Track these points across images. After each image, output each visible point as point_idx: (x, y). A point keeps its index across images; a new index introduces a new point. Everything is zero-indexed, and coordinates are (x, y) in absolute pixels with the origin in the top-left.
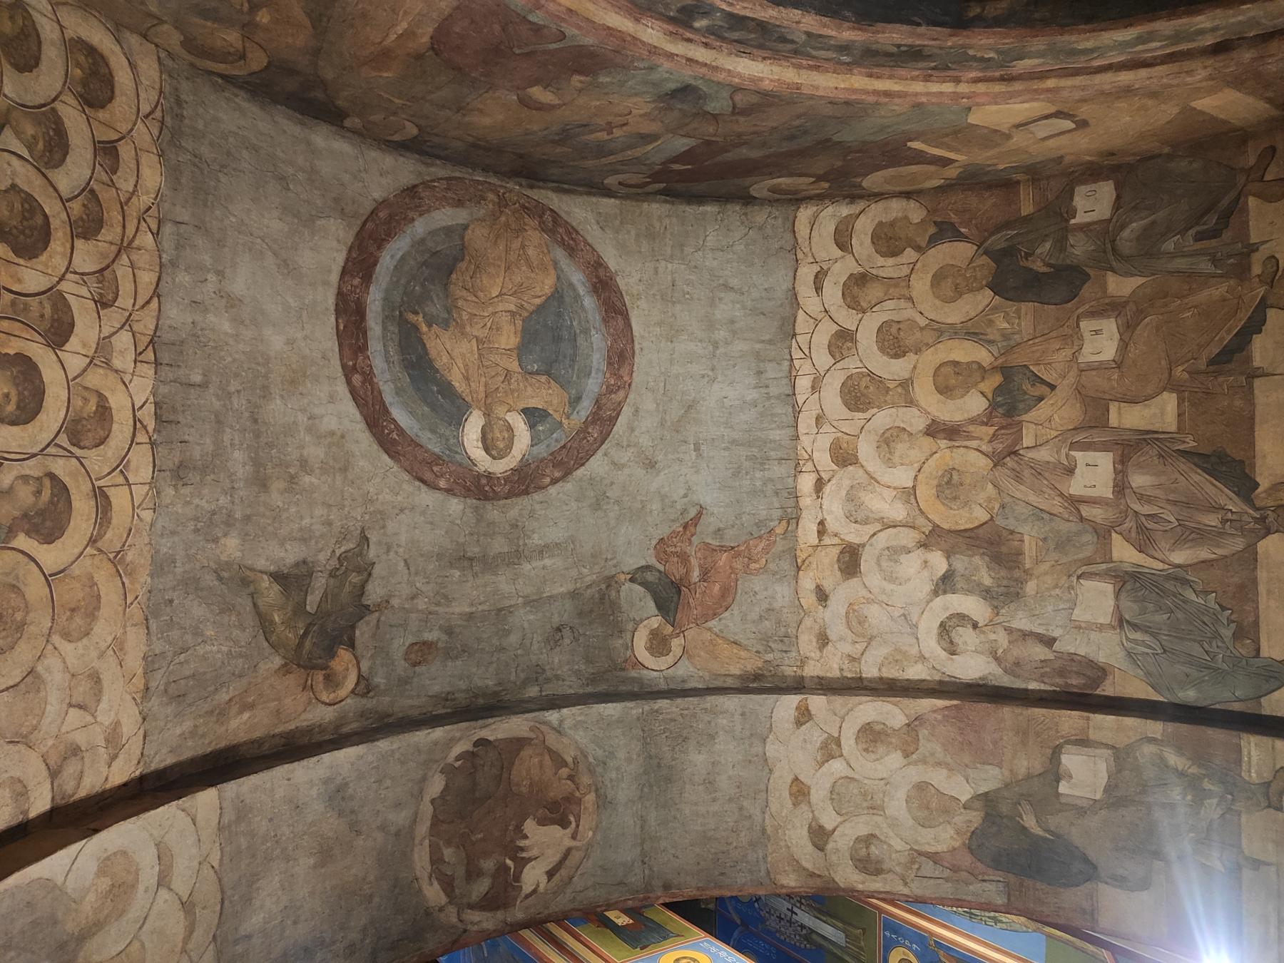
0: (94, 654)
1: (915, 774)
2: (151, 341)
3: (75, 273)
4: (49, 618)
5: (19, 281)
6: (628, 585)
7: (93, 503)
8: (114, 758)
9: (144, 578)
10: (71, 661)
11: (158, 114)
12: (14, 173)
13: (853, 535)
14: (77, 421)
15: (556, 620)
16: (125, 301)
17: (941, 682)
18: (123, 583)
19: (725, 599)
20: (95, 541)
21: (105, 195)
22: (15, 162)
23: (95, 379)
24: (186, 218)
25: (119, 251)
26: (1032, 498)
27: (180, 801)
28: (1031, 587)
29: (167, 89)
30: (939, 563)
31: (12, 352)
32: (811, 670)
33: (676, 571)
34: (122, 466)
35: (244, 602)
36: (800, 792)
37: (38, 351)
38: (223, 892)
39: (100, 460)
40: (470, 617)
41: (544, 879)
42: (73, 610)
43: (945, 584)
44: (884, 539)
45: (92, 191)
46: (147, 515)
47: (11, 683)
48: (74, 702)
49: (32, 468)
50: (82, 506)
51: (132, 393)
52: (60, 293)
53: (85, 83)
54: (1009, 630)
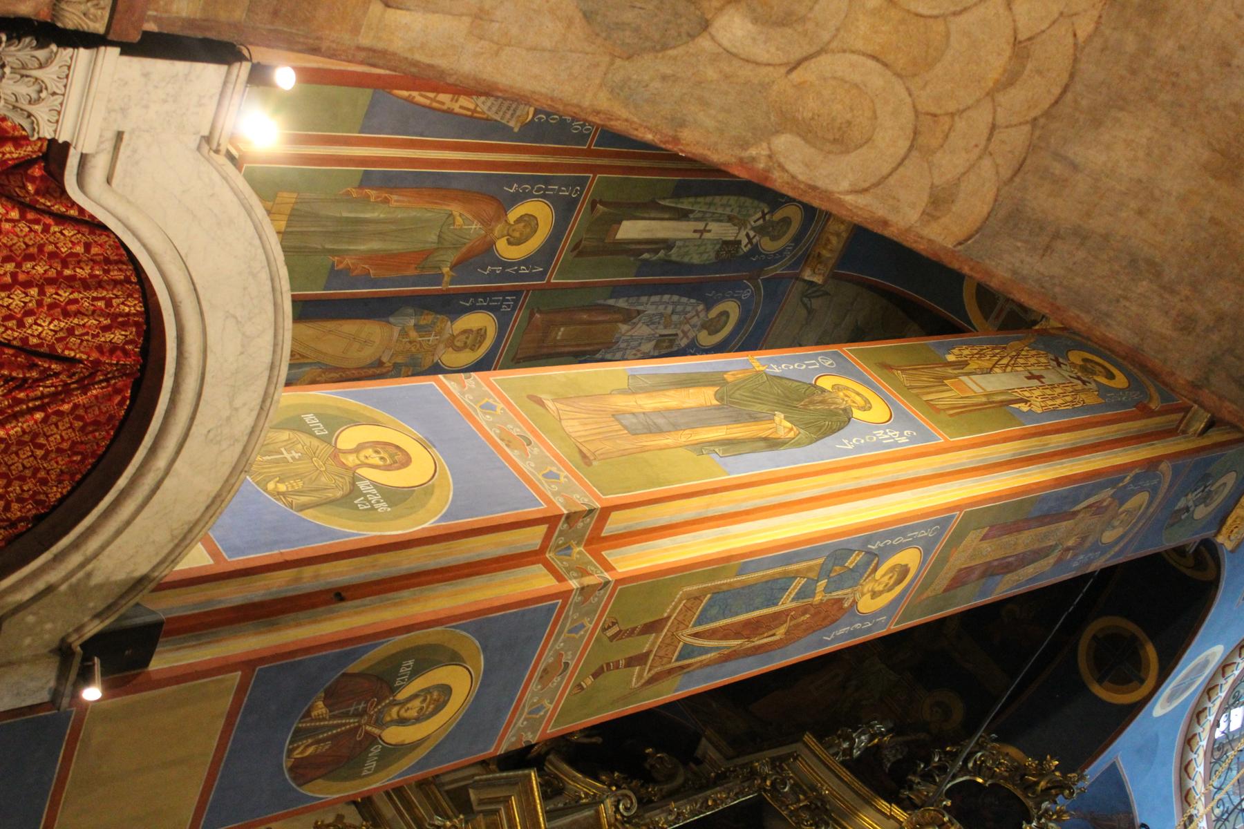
38: (1072, 76)
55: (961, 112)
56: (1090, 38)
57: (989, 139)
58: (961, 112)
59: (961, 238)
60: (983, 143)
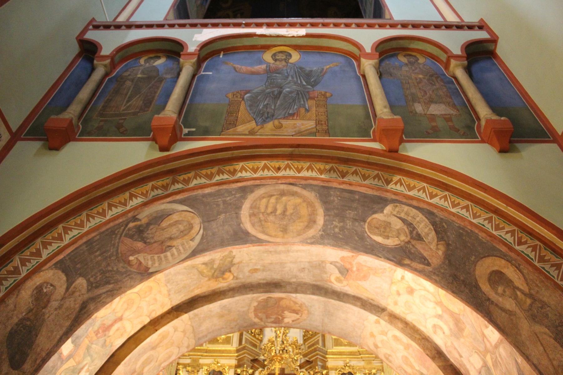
1: (406, 354)
6: (329, 264)
13: (413, 285)
15: (302, 266)
17: (429, 337)
19: (365, 278)
26: (473, 321)
28: (462, 340)
30: (440, 312)
32: (391, 307)
33: (348, 266)
35: (195, 271)
36: (372, 335)
40: (271, 264)
41: (291, 322)
43: (440, 317)
44: (423, 293)
54: (452, 343)
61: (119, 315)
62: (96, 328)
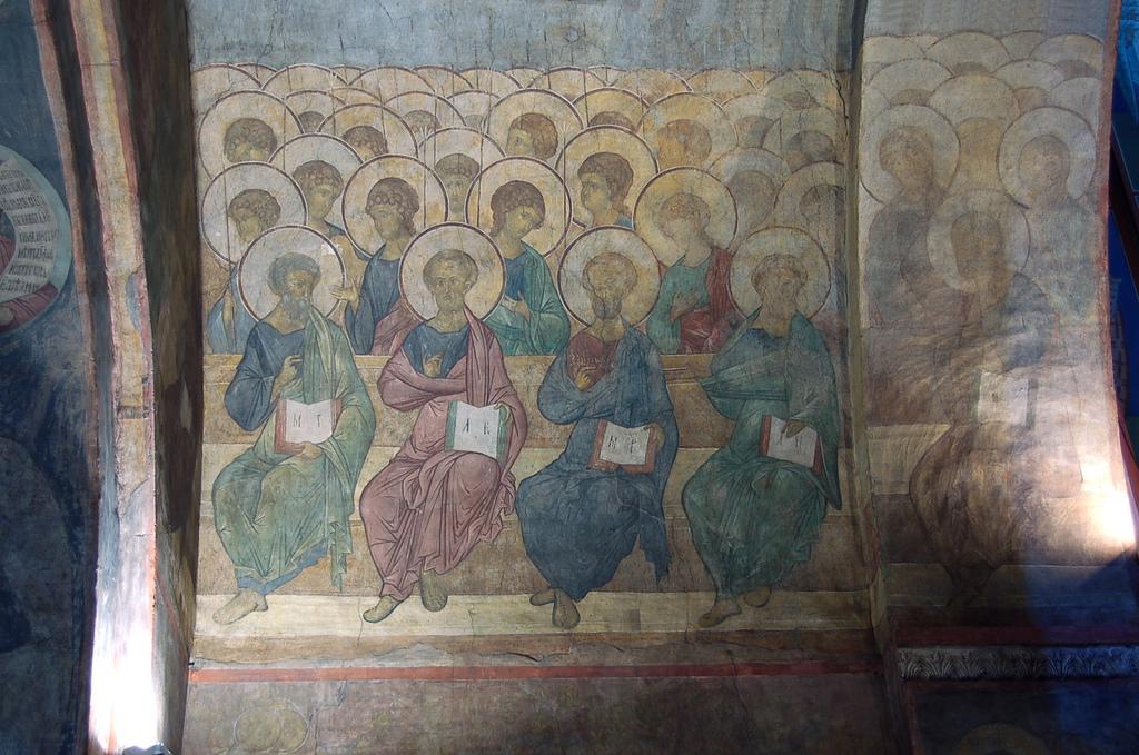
0: (724, 124)
2: (457, 74)
3: (417, 153)
4: (690, 172)
5: (437, 205)
7: (601, 132)
8: (813, 100)
9: (666, 76)
10: (724, 149)
11: (250, 70)
12: (358, 211)
14: (537, 150)
16: (427, 103)
18: (669, 97)
20: (633, 128)
21: (344, 127)
22: (348, 211)
23: (499, 134)
24: (336, 38)
25: (387, 110)
27: (864, 80)
29: (222, 60)
31: (492, 212)
34: (570, 102)
37: (488, 186)
38: (960, 32)
39: (566, 127)
42: (686, 148)
45: (345, 137)
46: (612, 75)
47: (732, 207)
48: (758, 144)
49: (576, 190)
50: (607, 141)
51: (508, 96)
52: (436, 166)
53: (260, 146)
55: (1011, 88)
56: (931, 33)
57: (1021, 60)
58: (1011, 88)
59: (1095, 42)
60: (1025, 63)
61: (699, 255)
62: (673, 342)
